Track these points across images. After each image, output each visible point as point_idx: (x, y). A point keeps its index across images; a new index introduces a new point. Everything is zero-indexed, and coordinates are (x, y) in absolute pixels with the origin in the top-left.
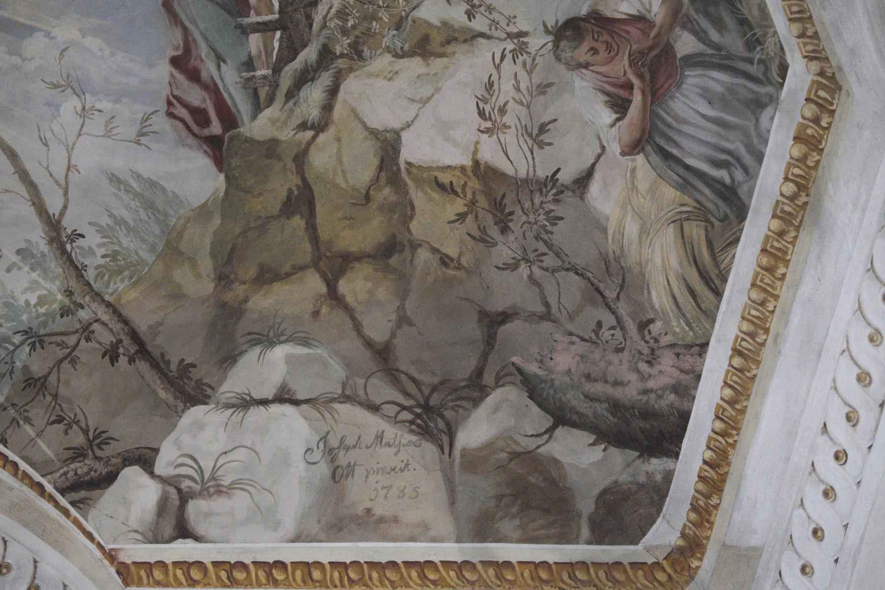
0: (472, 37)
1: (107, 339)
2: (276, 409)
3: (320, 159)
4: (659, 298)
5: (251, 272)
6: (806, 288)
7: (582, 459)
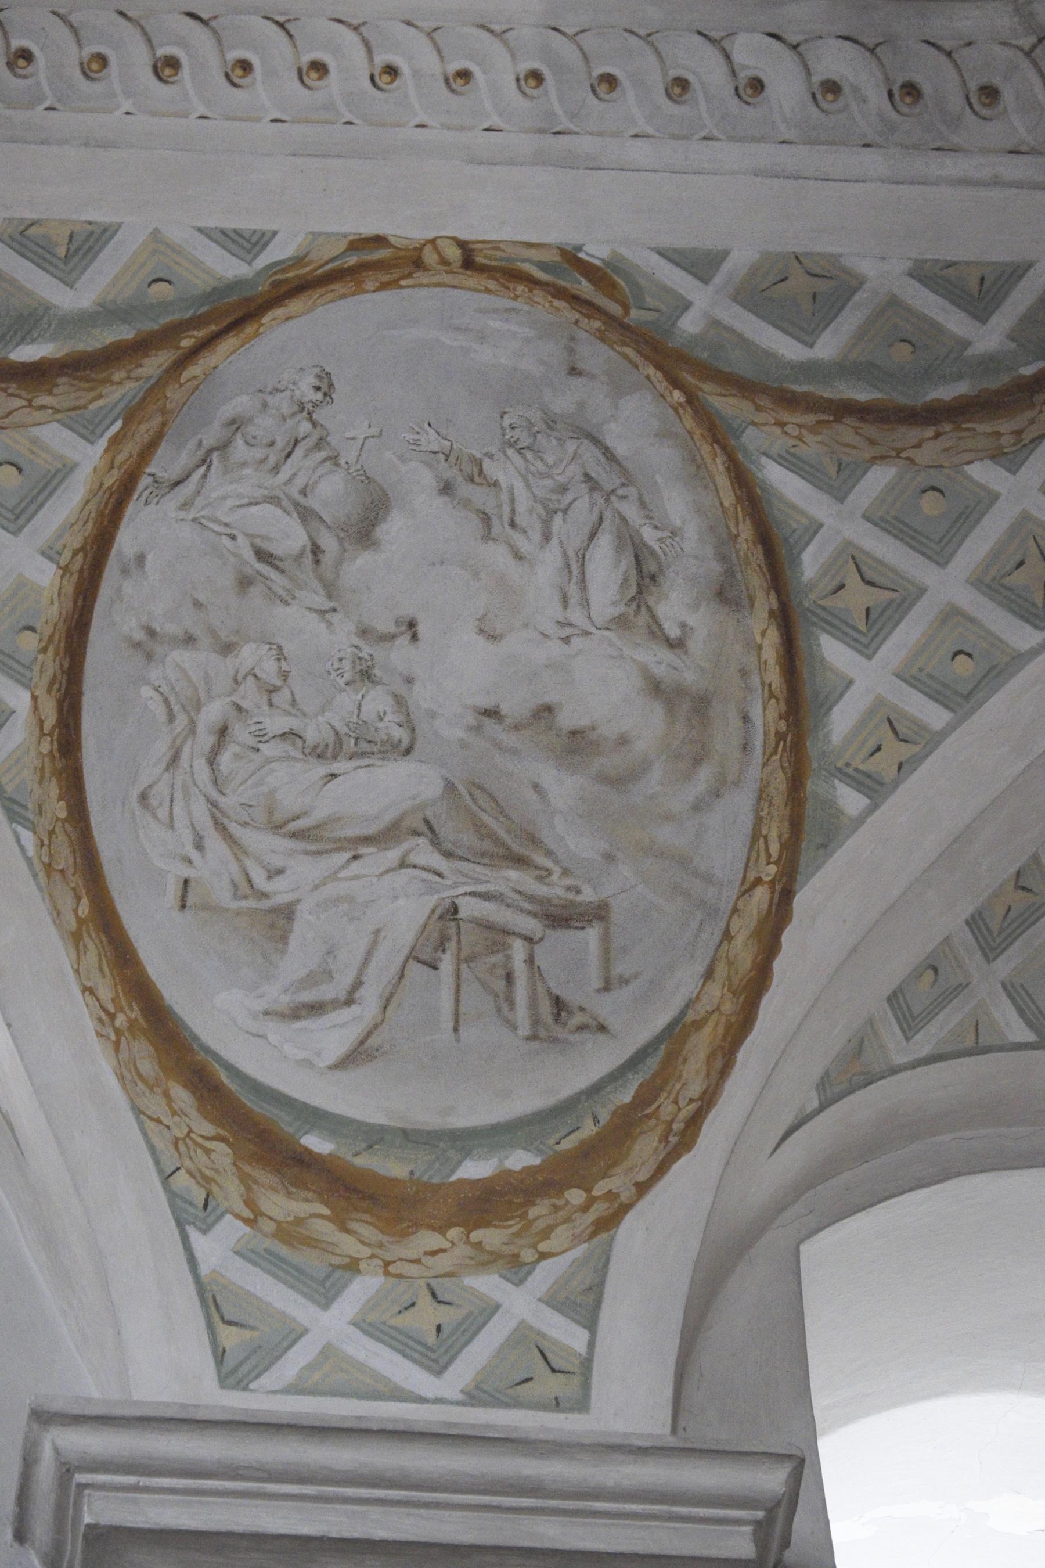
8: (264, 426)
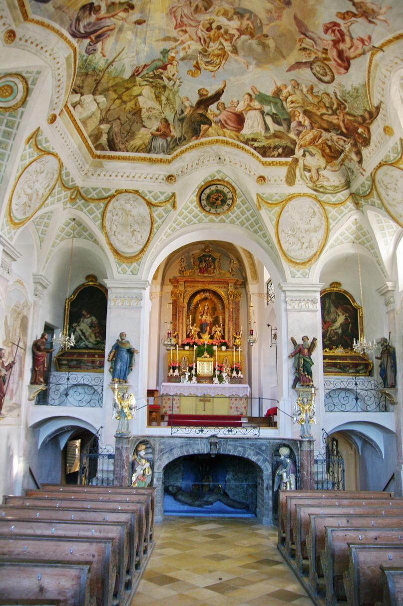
1: (98, 78)
3: (135, 88)
4: (132, 143)
5: (115, 89)
7: (104, 139)
8: (44, 162)
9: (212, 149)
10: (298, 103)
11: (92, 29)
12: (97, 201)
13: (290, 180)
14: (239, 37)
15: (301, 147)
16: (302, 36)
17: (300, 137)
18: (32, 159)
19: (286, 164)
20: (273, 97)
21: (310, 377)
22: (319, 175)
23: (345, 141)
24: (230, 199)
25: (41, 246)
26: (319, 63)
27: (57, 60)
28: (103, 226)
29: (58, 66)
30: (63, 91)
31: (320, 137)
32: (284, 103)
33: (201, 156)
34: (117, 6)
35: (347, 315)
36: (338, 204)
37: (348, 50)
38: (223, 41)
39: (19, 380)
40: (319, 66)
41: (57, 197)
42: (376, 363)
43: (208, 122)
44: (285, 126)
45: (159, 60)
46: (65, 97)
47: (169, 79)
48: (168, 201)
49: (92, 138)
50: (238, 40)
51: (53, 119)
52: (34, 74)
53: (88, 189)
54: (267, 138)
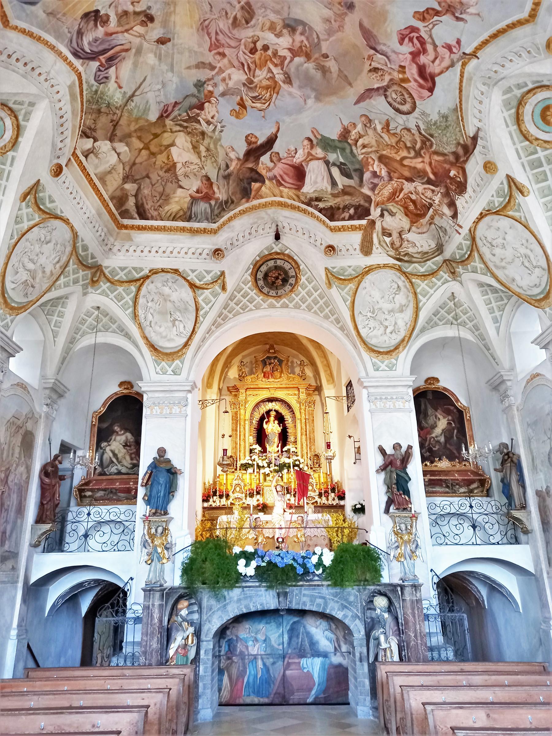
0: (200, 158)
1: (115, 118)
2: (116, 155)
3: (166, 135)
4: (167, 208)
5: (139, 135)
6: (181, 237)
8: (49, 228)
9: (267, 214)
10: (371, 147)
11: (101, 48)
12: (126, 284)
13: (366, 248)
14: (292, 60)
15: (378, 205)
16: (372, 52)
17: (376, 192)
18: (32, 223)
19: (359, 228)
20: (339, 141)
21: (407, 498)
22: (402, 239)
23: (433, 191)
24: (293, 277)
25: (54, 341)
26: (395, 88)
27: (56, 89)
28: (135, 316)
29: (59, 96)
30: (68, 133)
31: (402, 190)
32: (354, 148)
33: (254, 223)
34: (132, 18)
35: (450, 418)
36: (429, 275)
37: (431, 64)
38: (272, 67)
39: (16, 518)
40: (396, 92)
41: (72, 277)
42: (495, 478)
43: (260, 179)
44: (356, 178)
45: (193, 95)
46: (71, 142)
47: (208, 123)
48: (216, 281)
49: (115, 201)
50: (291, 64)
51: (58, 171)
52: (26, 105)
53: (114, 268)
54: (334, 196)
